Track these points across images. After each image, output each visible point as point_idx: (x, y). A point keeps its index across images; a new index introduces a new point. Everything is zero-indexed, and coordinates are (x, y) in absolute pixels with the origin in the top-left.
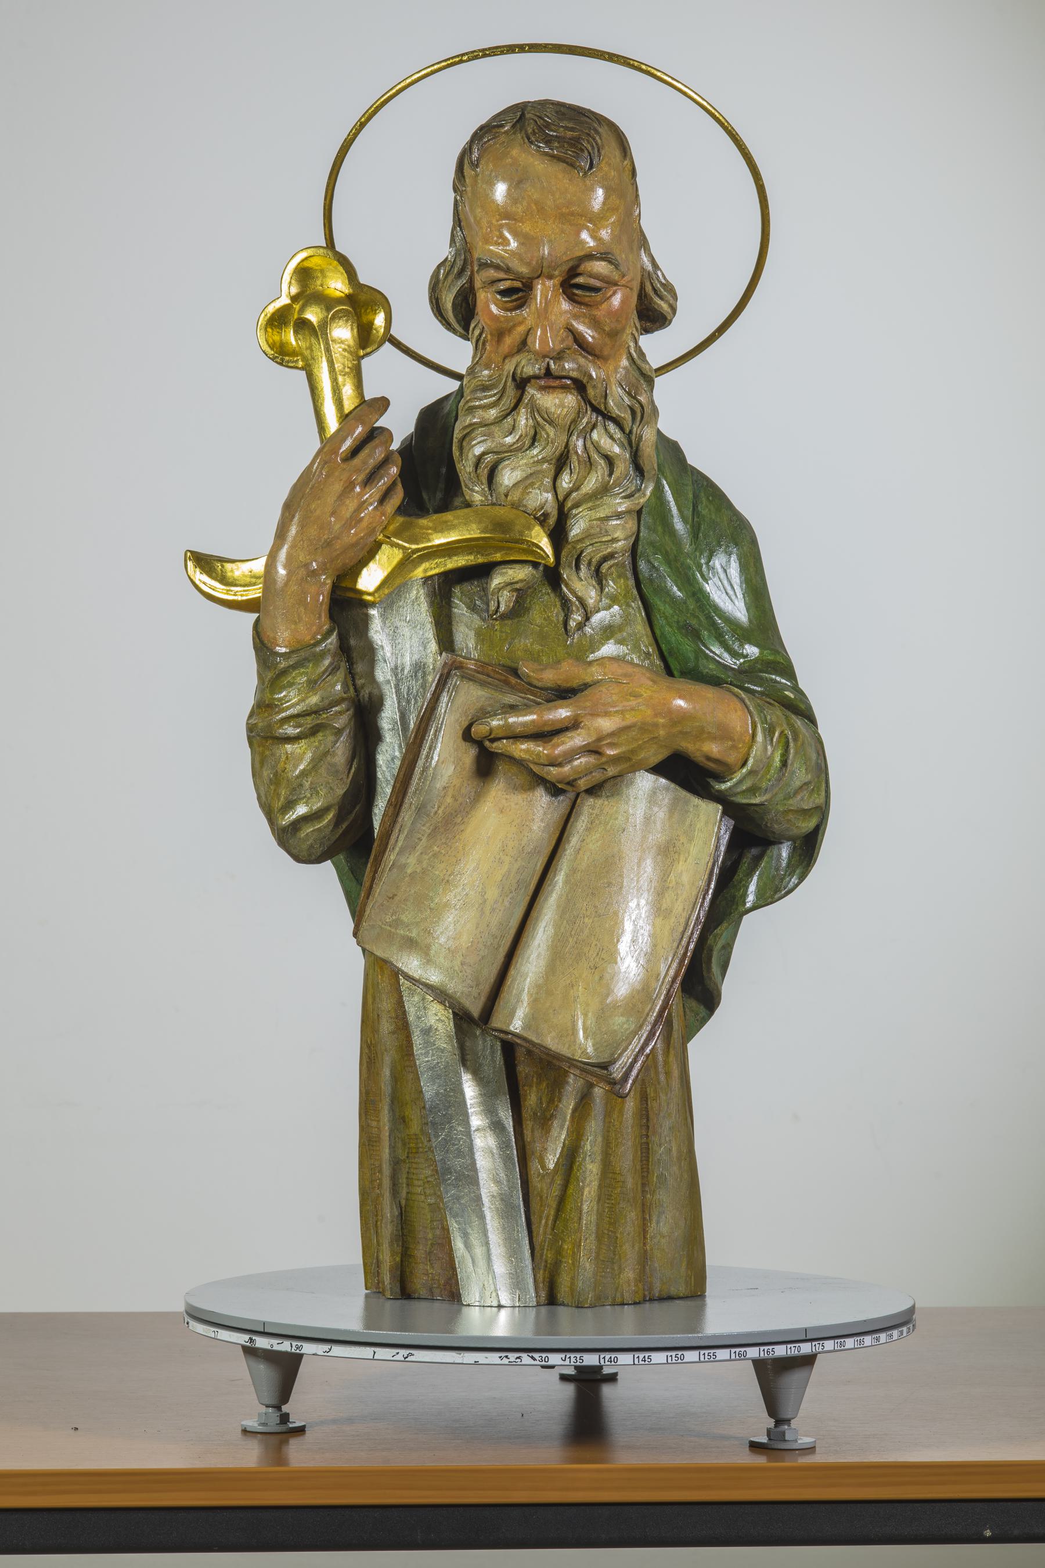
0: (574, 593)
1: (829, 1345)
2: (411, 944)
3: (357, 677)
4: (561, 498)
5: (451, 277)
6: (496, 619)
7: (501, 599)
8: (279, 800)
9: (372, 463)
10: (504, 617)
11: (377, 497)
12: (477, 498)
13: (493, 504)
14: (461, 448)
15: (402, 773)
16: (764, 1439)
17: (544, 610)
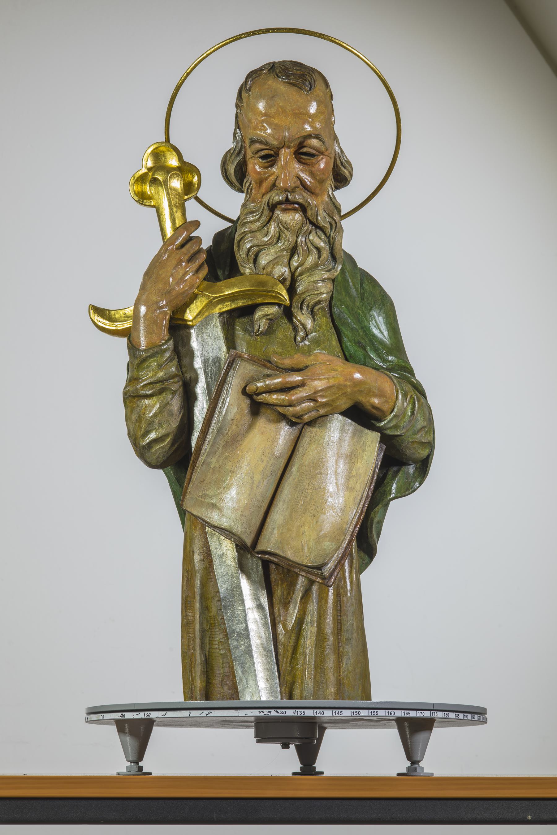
0: (299, 321)
1: (440, 714)
2: (214, 506)
3: (183, 367)
4: (293, 270)
5: (234, 156)
6: (258, 335)
7: (261, 324)
8: (141, 430)
9: (192, 251)
10: (262, 334)
11: (195, 269)
12: (248, 271)
13: (256, 274)
14: (239, 246)
15: (208, 415)
17: (284, 332)
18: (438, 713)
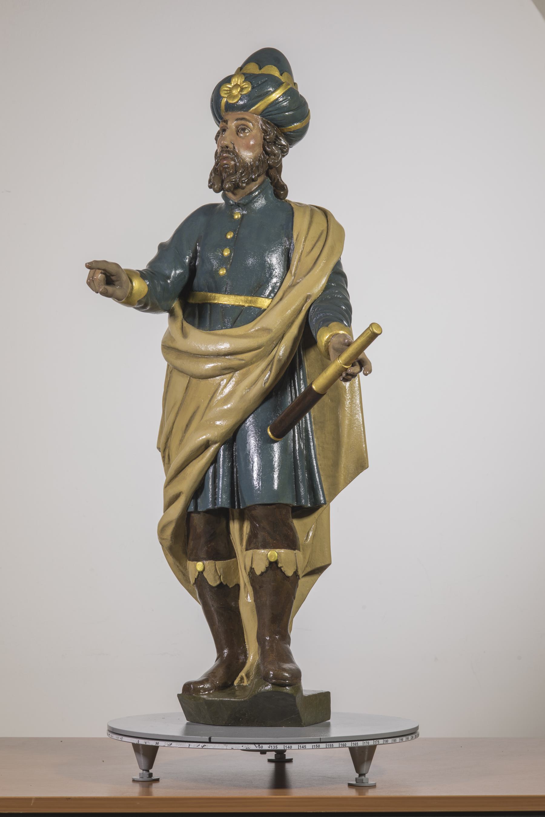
1: (381, 741)
16: (354, 782)
18: (380, 740)
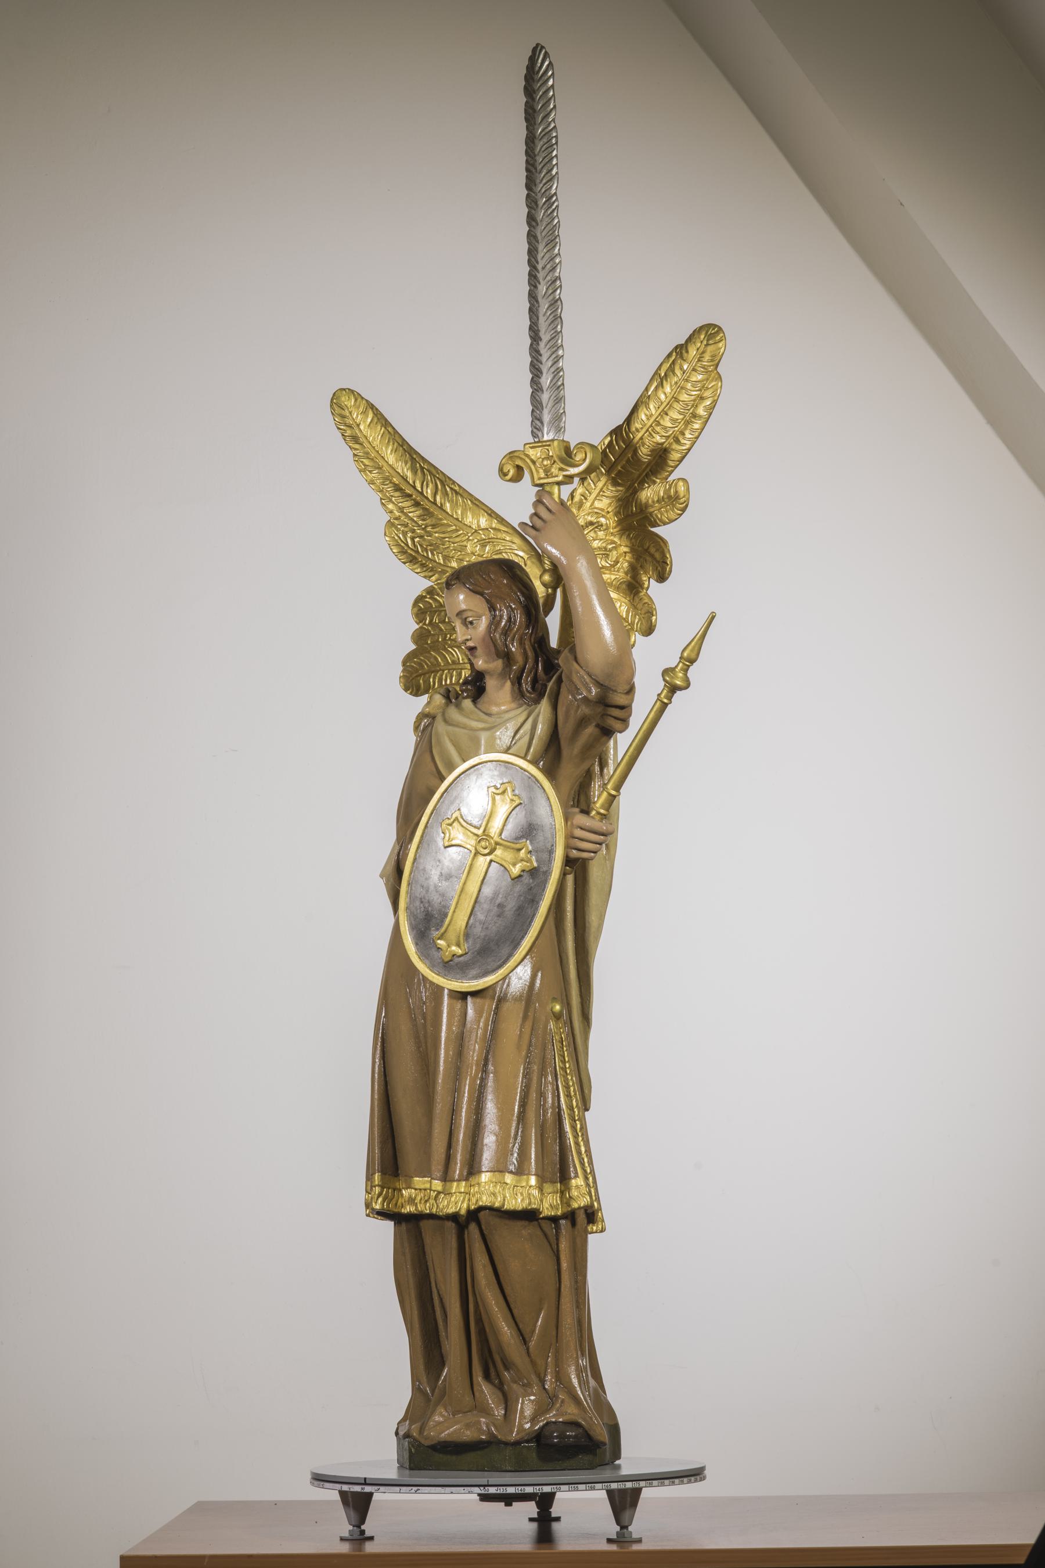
1: (642, 1484)
